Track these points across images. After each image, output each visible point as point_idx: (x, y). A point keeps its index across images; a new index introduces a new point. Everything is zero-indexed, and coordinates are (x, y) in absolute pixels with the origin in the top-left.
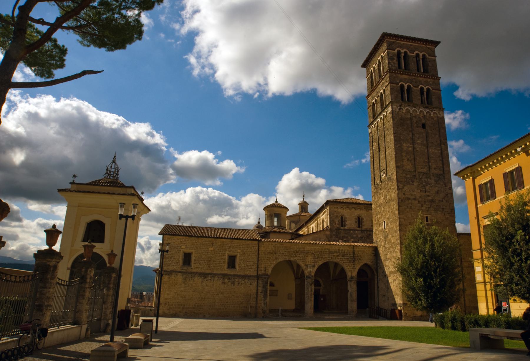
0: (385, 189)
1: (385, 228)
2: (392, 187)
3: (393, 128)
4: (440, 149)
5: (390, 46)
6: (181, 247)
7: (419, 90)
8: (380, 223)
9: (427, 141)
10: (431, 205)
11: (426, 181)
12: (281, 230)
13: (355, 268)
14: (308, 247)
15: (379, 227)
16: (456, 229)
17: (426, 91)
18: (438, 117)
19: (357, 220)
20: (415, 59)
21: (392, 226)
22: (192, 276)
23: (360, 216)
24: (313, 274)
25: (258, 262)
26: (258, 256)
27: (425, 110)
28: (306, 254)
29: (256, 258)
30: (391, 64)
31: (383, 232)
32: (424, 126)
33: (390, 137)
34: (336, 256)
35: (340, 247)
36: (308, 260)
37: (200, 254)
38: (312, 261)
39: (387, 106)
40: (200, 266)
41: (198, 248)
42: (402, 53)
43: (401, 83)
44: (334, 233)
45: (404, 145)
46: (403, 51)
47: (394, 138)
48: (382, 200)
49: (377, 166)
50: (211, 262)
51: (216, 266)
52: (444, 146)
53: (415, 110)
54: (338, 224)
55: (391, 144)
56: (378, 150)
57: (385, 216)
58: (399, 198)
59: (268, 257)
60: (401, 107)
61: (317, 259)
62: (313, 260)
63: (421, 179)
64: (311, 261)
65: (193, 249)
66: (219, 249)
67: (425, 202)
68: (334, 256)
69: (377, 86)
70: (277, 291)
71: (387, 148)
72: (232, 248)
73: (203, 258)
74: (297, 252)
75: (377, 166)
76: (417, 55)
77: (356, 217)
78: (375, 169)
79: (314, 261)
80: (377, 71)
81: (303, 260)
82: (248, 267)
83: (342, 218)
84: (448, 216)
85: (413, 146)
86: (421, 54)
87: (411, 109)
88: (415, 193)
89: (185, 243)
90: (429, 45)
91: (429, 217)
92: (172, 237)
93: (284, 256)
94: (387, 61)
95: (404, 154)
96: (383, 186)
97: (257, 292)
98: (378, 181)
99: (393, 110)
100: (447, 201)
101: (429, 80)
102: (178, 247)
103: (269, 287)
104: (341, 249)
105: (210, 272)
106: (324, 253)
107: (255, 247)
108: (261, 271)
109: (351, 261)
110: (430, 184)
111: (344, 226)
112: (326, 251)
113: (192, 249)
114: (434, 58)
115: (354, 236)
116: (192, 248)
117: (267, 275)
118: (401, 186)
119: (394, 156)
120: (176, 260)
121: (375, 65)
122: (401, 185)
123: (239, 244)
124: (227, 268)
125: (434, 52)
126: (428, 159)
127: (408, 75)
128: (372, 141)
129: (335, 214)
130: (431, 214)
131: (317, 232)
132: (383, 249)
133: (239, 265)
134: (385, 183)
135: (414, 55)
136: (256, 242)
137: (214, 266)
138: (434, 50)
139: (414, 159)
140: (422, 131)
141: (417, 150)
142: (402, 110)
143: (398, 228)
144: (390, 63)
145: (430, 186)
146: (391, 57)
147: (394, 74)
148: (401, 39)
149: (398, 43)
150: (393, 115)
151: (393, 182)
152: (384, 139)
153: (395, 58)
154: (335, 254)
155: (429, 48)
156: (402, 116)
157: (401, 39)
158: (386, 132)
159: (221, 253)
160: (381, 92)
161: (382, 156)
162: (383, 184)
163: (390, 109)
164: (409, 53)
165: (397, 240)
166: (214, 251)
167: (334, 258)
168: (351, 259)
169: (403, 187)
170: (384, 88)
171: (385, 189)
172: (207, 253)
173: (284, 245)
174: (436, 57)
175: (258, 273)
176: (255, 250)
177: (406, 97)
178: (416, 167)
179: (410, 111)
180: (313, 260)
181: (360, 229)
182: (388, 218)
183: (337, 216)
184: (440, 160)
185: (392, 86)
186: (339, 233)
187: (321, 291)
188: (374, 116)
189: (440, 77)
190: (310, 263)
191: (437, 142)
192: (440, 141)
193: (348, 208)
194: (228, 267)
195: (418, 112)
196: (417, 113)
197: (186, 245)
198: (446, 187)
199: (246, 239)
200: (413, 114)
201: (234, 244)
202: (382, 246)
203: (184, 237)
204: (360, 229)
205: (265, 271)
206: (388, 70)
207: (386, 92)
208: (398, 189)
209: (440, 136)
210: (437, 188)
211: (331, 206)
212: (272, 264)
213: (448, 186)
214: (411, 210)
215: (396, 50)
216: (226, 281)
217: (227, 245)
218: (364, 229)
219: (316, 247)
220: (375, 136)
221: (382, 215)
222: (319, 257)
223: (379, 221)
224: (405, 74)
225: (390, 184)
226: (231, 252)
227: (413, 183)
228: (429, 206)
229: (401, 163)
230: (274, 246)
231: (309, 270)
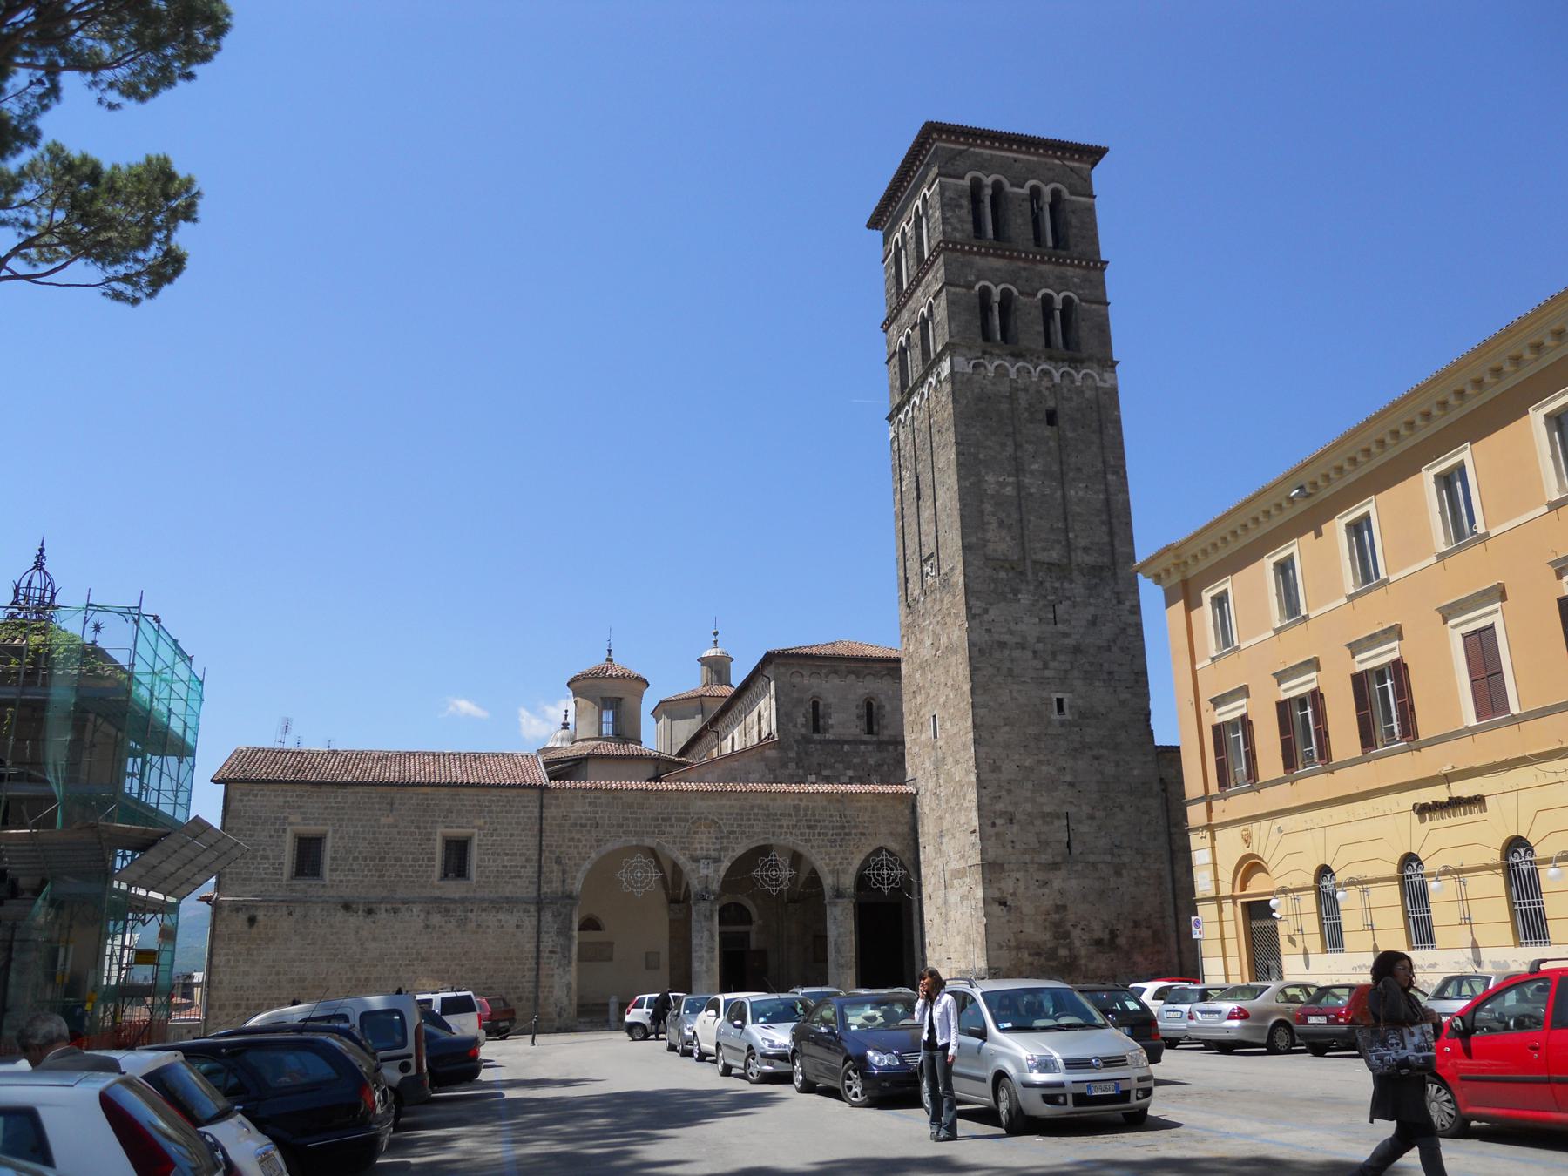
0: (935, 615)
1: (935, 737)
2: (954, 611)
3: (955, 426)
4: (1103, 487)
5: (949, 165)
7: (1040, 303)
9: (1061, 463)
10: (1071, 663)
11: (1057, 589)
12: (622, 750)
13: (850, 864)
14: (699, 803)
16: (1151, 733)
17: (1061, 307)
18: (1097, 388)
19: (864, 711)
20: (1029, 204)
21: (955, 730)
23: (873, 699)
24: (715, 887)
25: (540, 855)
26: (541, 837)
27: (1055, 368)
28: (693, 823)
29: (535, 841)
30: (950, 224)
31: (930, 749)
32: (1051, 417)
33: (947, 457)
34: (788, 827)
35: (801, 800)
36: (700, 843)
37: (349, 838)
38: (713, 847)
39: (939, 358)
40: (350, 878)
41: (343, 820)
42: (987, 186)
43: (981, 283)
44: (792, 754)
45: (990, 478)
46: (989, 181)
47: (958, 459)
48: (926, 652)
49: (912, 544)
50: (387, 862)
51: (403, 874)
52: (1114, 478)
53: (1024, 367)
54: (803, 725)
55: (949, 476)
56: (915, 494)
57: (935, 700)
58: (971, 645)
59: (572, 840)
60: (982, 360)
61: (728, 838)
62: (714, 844)
63: (1041, 583)
64: (710, 846)
65: (327, 825)
66: (412, 822)
67: (1054, 654)
68: (781, 827)
69: (912, 294)
70: (611, 944)
71: (938, 487)
72: (454, 814)
73: (360, 853)
74: (663, 820)
75: (912, 544)
76: (1035, 193)
77: (861, 703)
79: (718, 846)
80: (912, 245)
81: (684, 843)
83: (815, 705)
84: (1125, 696)
85: (1018, 482)
86: (1047, 190)
87: (1013, 366)
88: (1021, 627)
89: (299, 807)
90: (1072, 158)
91: (1066, 701)
92: (257, 787)
93: (624, 833)
94: (938, 214)
95: (988, 508)
96: (929, 606)
97: (538, 951)
98: (917, 592)
99: (956, 370)
100: (1122, 649)
101: (1070, 271)
102: (276, 818)
103: (575, 933)
104: (803, 804)
106: (749, 820)
107: (530, 809)
108: (550, 882)
109: (835, 841)
110: (1069, 598)
111: (822, 731)
112: (755, 814)
114: (1091, 200)
115: (856, 761)
116: (325, 819)
117: (570, 896)
118: (978, 605)
119: (956, 513)
120: (271, 861)
121: (907, 224)
122: (978, 603)
123: (478, 801)
124: (441, 879)
125: (1087, 181)
126: (1066, 519)
127: (1003, 256)
128: (900, 466)
129: (795, 695)
130: (1072, 692)
131: (744, 751)
133: (479, 867)
134: (933, 597)
135: (1026, 191)
136: (535, 794)
137: (397, 875)
138: (1090, 176)
139: (1021, 520)
140: (1047, 433)
141: (1031, 494)
142: (983, 369)
143: (971, 735)
144: (948, 218)
145: (1068, 602)
146: (951, 198)
147: (959, 254)
148: (983, 141)
149: (977, 154)
150: (953, 383)
151: (954, 596)
152: (930, 459)
153: (965, 202)
154: (785, 822)
155: (1072, 169)
156: (982, 389)
157: (983, 141)
158: (936, 438)
159: (420, 834)
160: (923, 312)
161: (927, 514)
162: (928, 600)
163: (945, 367)
164: (1008, 187)
165: (968, 773)
166: (396, 826)
167: (781, 833)
168: (836, 834)
169: (986, 611)
170: (931, 299)
171: (935, 615)
172: (374, 833)
173: (621, 798)
174: (1095, 197)
175: (539, 890)
176: (530, 818)
177: (998, 327)
178: (1027, 545)
179: (1007, 370)
180: (714, 844)
181: (875, 738)
183: (800, 701)
184: (1103, 523)
185: (954, 293)
186: (806, 754)
187: (753, 937)
188: (904, 385)
189: (1107, 262)
190: (705, 853)
191: (1093, 466)
192: (1104, 462)
193: (835, 672)
194: (445, 876)
195: (1035, 374)
196: (1030, 377)
198: (1121, 607)
199: (498, 786)
200: (1020, 381)
203: (297, 788)
204: (875, 738)
205: (564, 881)
206: (941, 241)
207: (935, 311)
208: (971, 616)
209: (1102, 447)
210: (1092, 610)
211: (782, 670)
212: (584, 859)
213: (1128, 603)
214: (1010, 678)
215: (968, 177)
216: (436, 919)
217: (437, 805)
218: (885, 738)
219: (724, 802)
220: (907, 451)
221: (929, 694)
222: (735, 832)
223: (921, 713)
224: (995, 255)
225: (947, 599)
226: (452, 827)
227: (1016, 595)
228: (1068, 666)
229: (980, 535)
230: (590, 803)
231: (704, 872)
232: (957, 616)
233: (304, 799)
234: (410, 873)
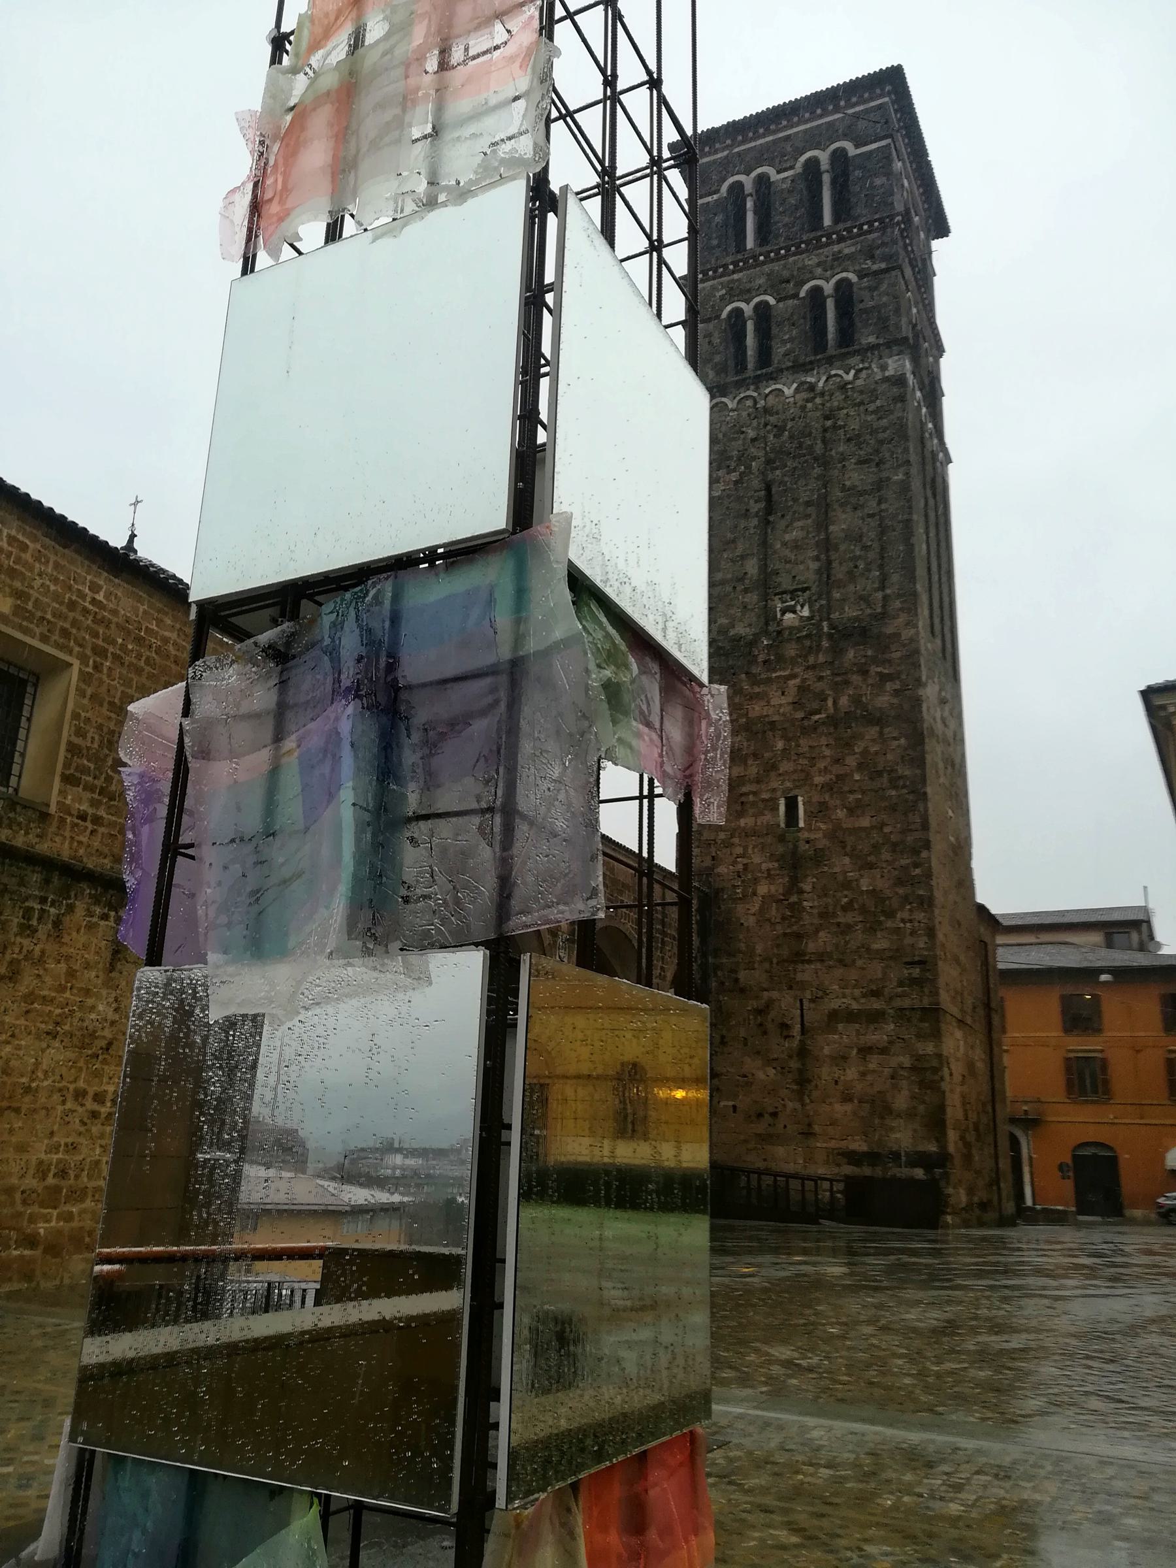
8: (743, 799)
40: (102, 812)
121: (778, 172)
182: (828, 787)
221: (774, 767)
232: (884, 678)
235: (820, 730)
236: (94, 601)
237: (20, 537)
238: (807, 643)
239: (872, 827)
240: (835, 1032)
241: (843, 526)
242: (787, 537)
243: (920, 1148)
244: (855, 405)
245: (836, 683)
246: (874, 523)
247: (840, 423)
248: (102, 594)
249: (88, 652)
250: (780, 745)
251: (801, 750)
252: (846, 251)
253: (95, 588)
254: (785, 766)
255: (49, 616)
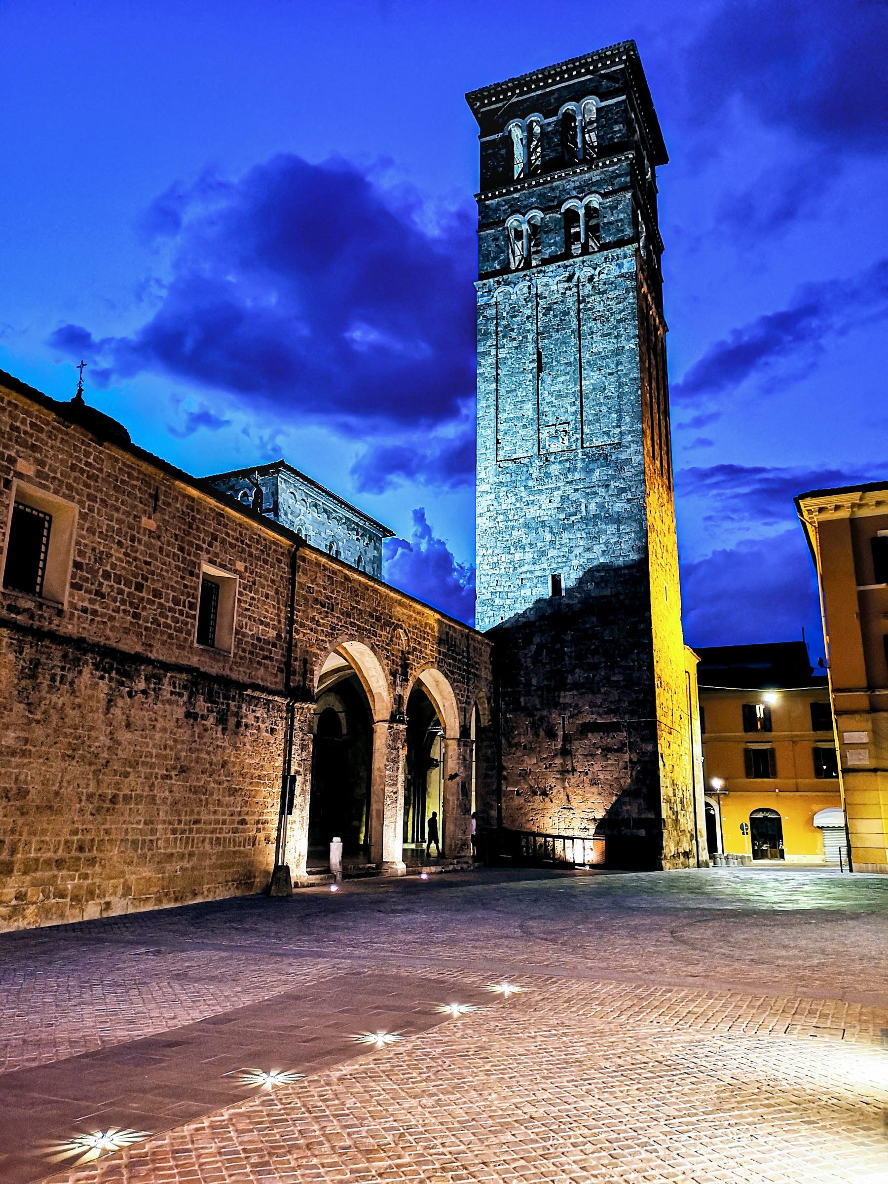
6: (12, 460)
15: (522, 586)
22: (65, 656)
40: (97, 607)
50: (144, 594)
73: (113, 566)
78: (503, 416)
82: (262, 649)
89: (34, 448)
105: (139, 649)
113: (65, 496)
123: (241, 534)
132: (538, 652)
133: (237, 633)
166: (159, 537)
193: (316, 506)
197: (41, 463)
201: (225, 526)
202: (534, 648)
216: (201, 705)
223: (524, 569)
233: (43, 436)
234: (169, 621)
235: (576, 527)
236: (87, 464)
237: (39, 423)
238: (567, 465)
239: (612, 596)
240: (586, 737)
241: (592, 381)
242: (553, 388)
243: (643, 816)
244: (599, 293)
245: (588, 494)
246: (612, 379)
247: (589, 306)
248: (92, 457)
249: (85, 499)
250: (548, 537)
251: (563, 542)
252: (594, 179)
253: (87, 454)
254: (552, 553)
255: (59, 475)
